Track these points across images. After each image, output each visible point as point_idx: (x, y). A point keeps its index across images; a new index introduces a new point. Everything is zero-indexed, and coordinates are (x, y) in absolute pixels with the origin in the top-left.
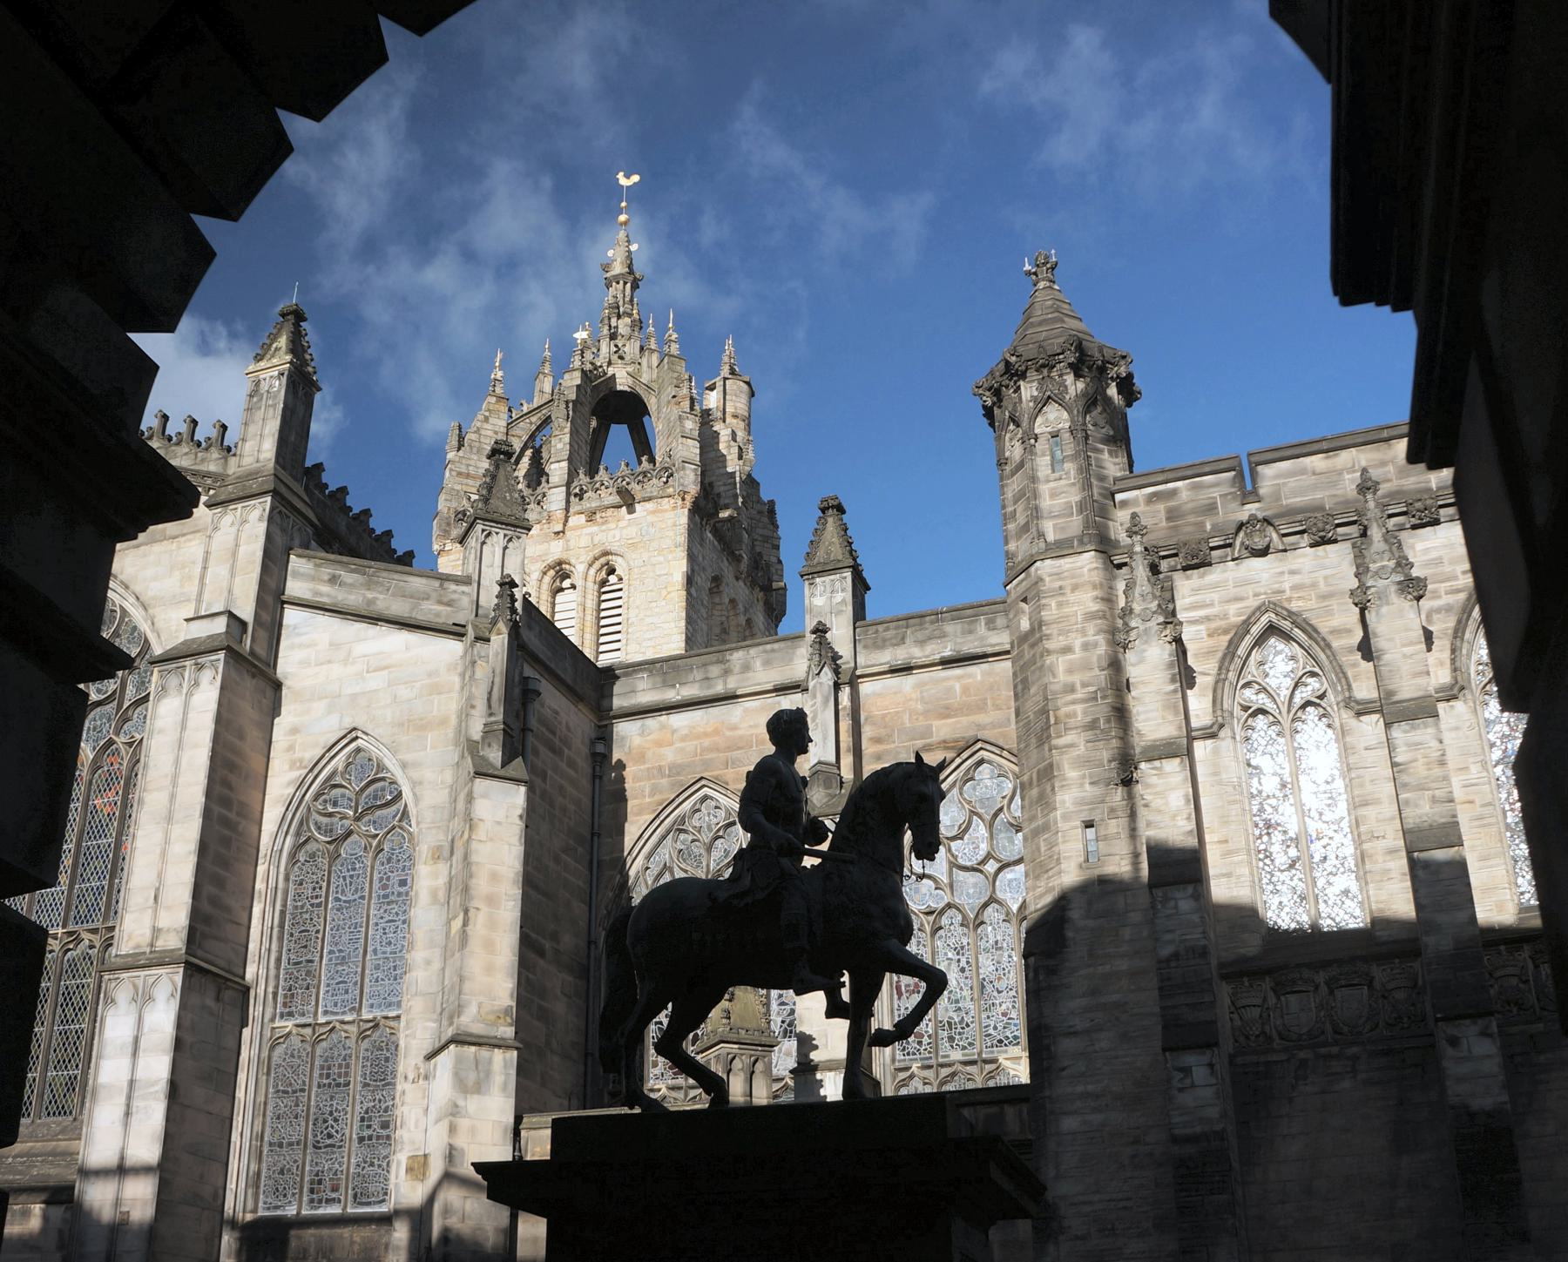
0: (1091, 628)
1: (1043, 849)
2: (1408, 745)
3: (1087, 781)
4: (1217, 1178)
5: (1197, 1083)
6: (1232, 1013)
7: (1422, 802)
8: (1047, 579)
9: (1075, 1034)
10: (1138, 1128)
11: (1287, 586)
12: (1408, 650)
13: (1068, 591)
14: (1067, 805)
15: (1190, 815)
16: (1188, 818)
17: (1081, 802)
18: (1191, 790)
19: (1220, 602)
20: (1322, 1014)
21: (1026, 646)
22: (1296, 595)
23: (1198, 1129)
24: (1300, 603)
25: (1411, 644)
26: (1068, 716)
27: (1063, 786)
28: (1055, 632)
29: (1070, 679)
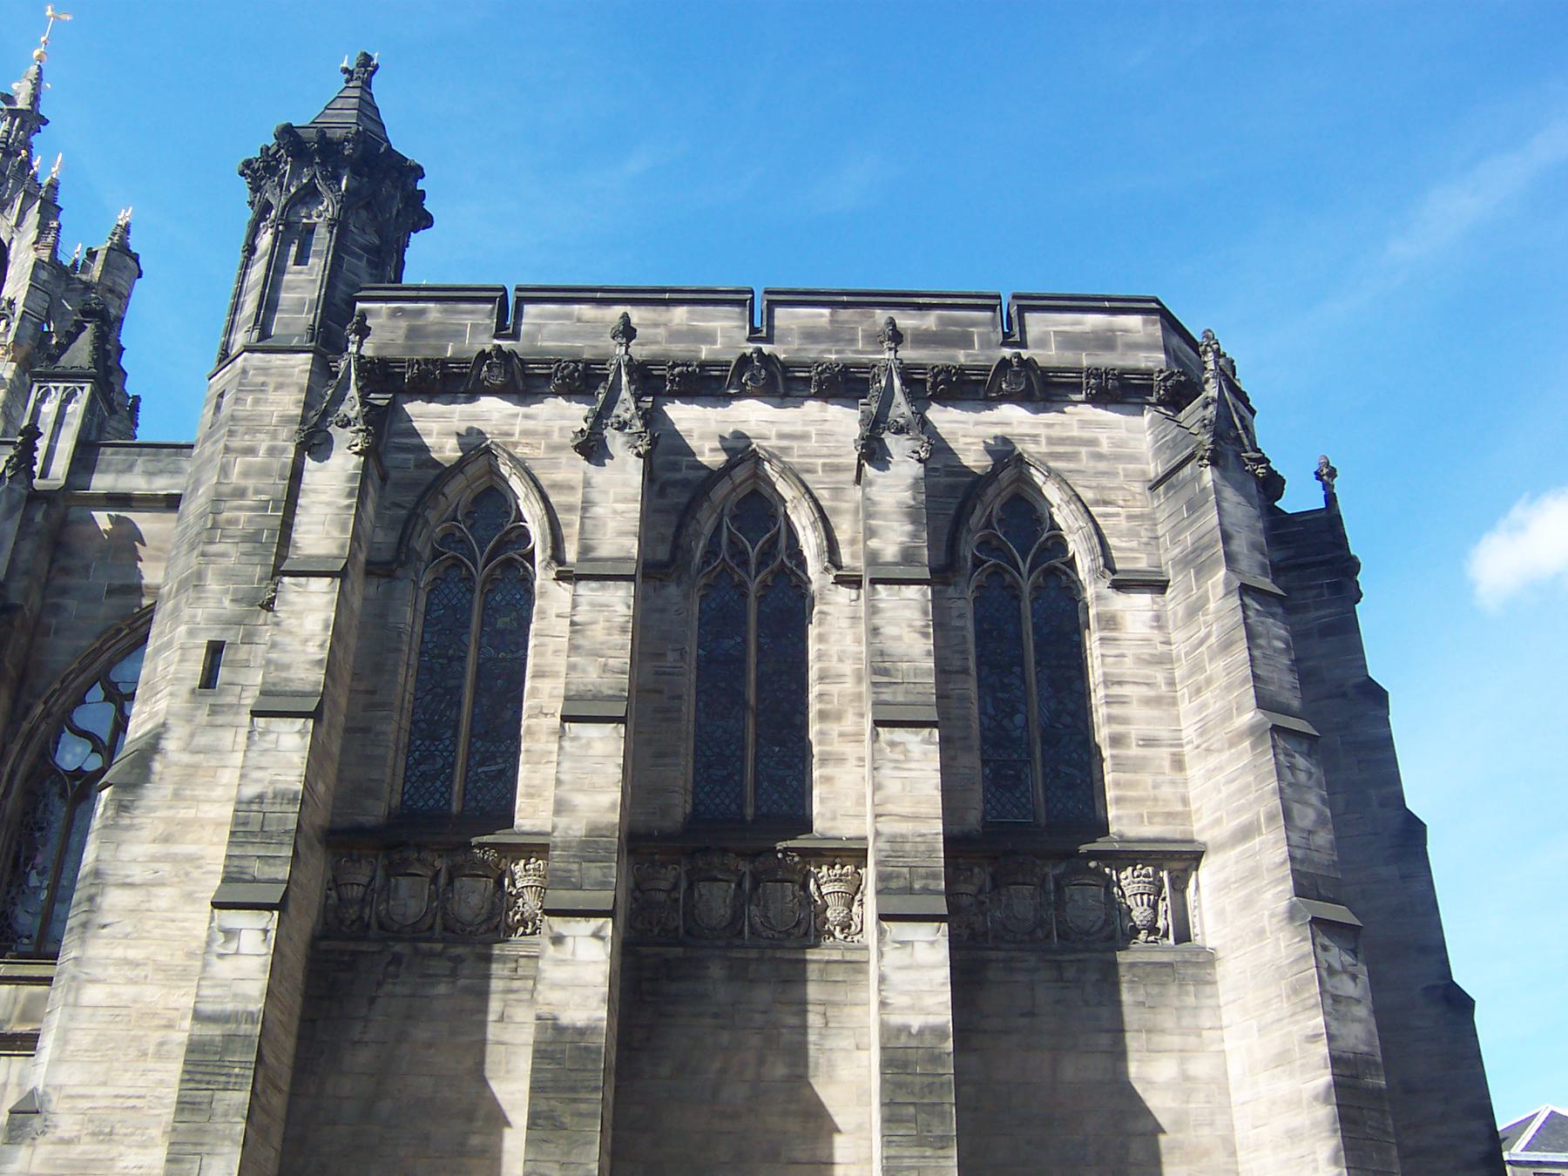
0: (284, 433)
1: (160, 669)
2: (593, 605)
3: (229, 597)
4: (237, 1070)
5: (243, 950)
6: (330, 889)
7: (591, 669)
8: (251, 372)
9: (131, 885)
10: (177, 1009)
11: (517, 430)
12: (620, 507)
13: (270, 388)
14: (198, 620)
15: (325, 642)
16: (322, 646)
17: (216, 620)
18: (333, 615)
19: (439, 434)
20: (435, 904)
21: (208, 444)
22: (524, 441)
23: (230, 1007)
24: (526, 450)
25: (625, 500)
26: (230, 522)
27: (200, 598)
28: (242, 429)
29: (243, 483)
